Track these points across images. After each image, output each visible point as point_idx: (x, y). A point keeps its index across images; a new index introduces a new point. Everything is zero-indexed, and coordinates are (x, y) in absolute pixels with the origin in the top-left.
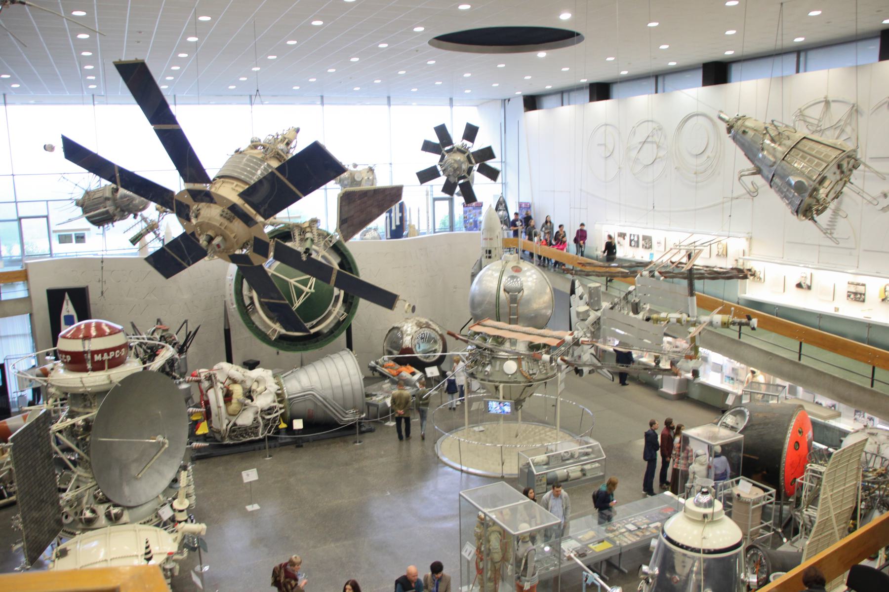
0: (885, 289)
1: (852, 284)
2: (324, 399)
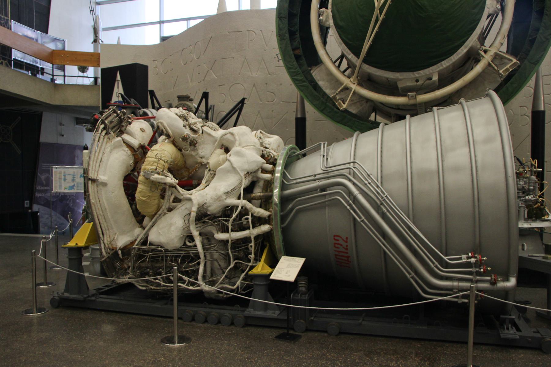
2: (377, 208)
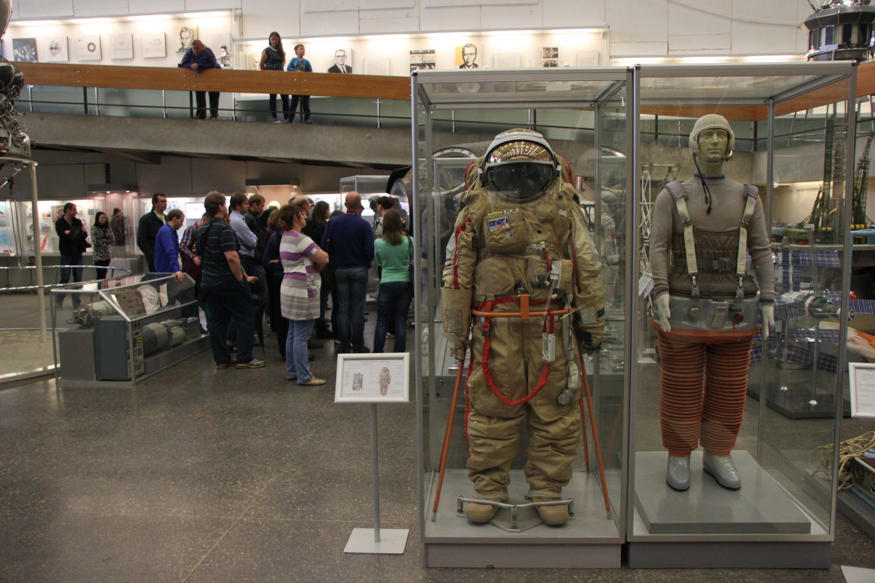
0: (463, 52)
1: (417, 53)
